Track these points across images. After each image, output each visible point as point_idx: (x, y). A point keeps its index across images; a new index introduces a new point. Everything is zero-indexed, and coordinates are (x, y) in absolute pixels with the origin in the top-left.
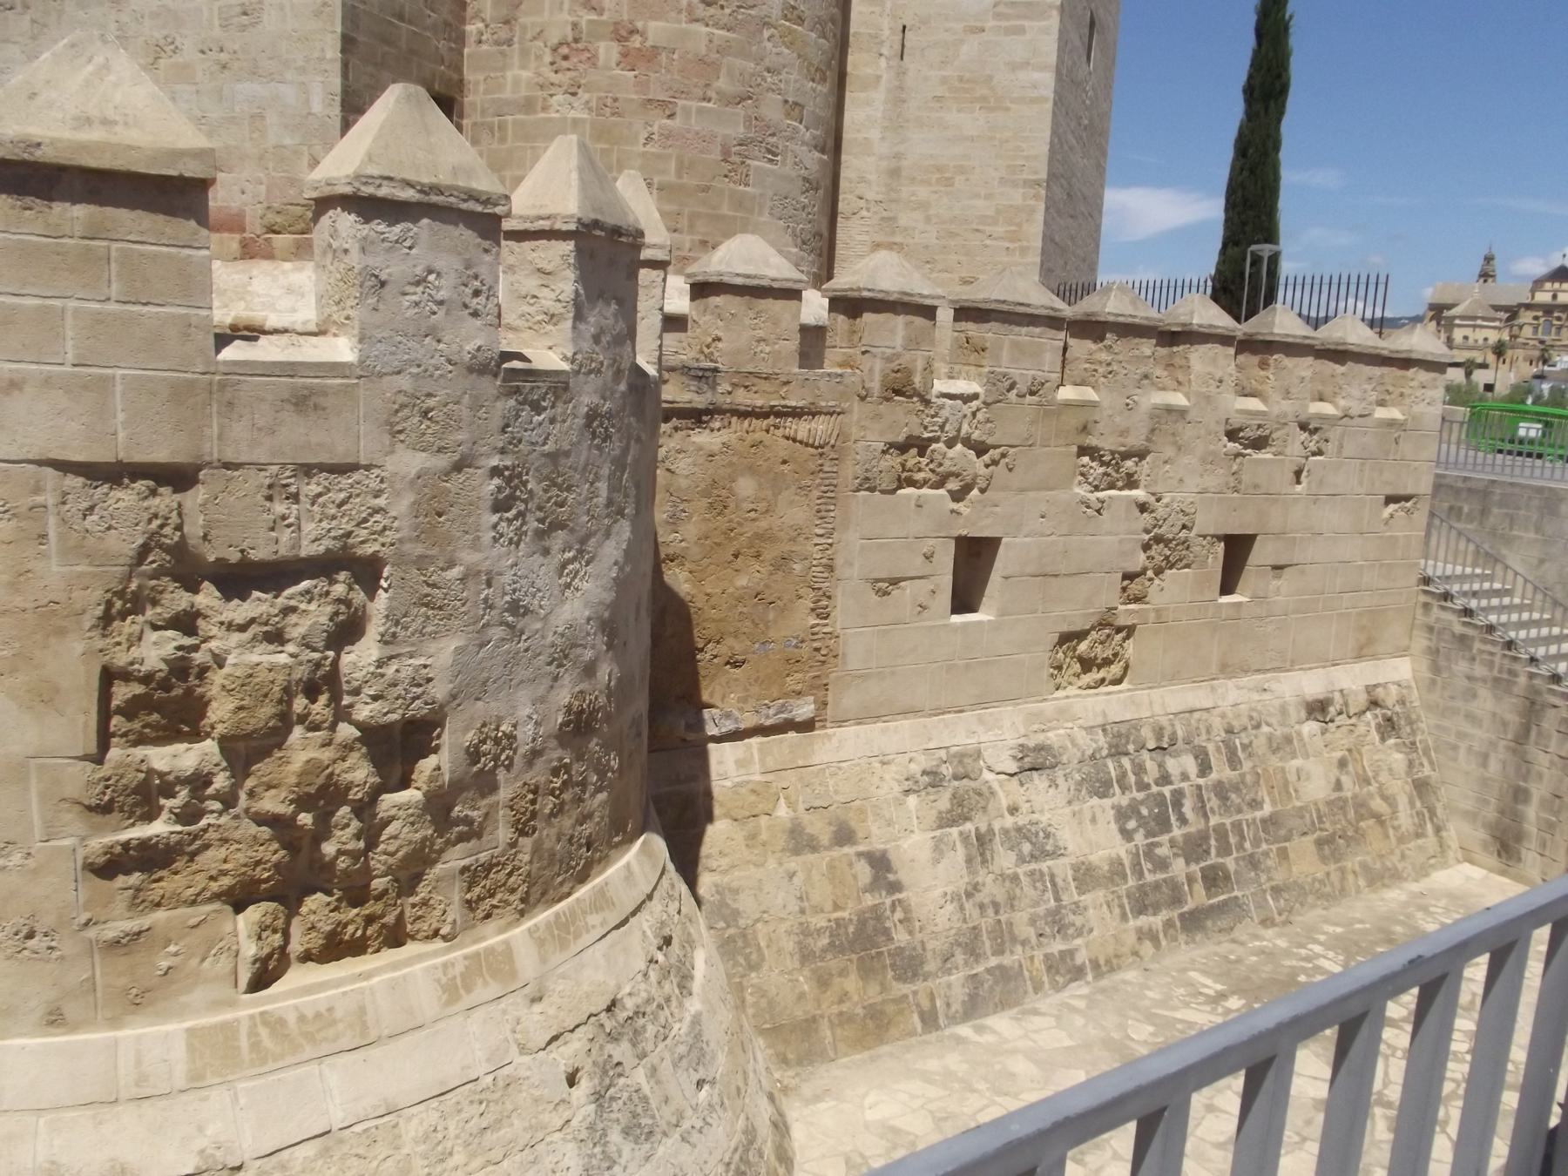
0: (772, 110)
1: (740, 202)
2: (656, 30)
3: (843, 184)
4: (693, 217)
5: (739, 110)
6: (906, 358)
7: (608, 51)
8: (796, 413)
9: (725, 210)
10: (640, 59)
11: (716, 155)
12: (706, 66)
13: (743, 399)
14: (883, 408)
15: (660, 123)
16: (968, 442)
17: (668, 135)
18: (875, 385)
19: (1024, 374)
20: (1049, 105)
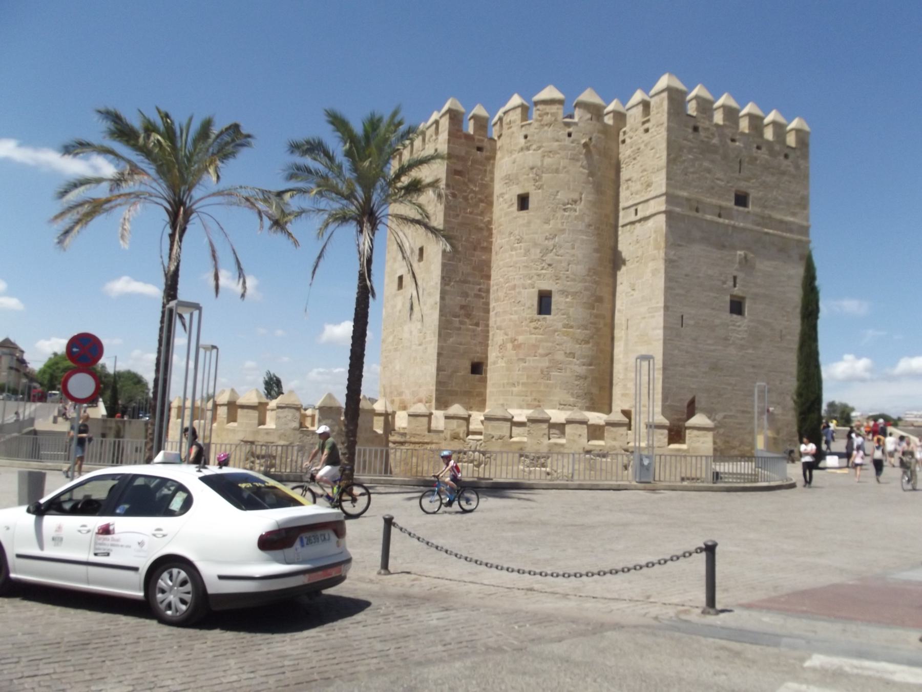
0: (560, 356)
1: (547, 386)
2: (521, 339)
3: (615, 375)
4: (531, 392)
5: (546, 358)
6: (457, 430)
7: (509, 346)
8: (427, 443)
9: (542, 388)
10: (517, 347)
11: (539, 372)
12: (535, 347)
13: (413, 440)
14: (452, 443)
15: (522, 365)
16: (479, 452)
17: (524, 368)
18: (448, 437)
19: (496, 434)
20: (661, 342)
